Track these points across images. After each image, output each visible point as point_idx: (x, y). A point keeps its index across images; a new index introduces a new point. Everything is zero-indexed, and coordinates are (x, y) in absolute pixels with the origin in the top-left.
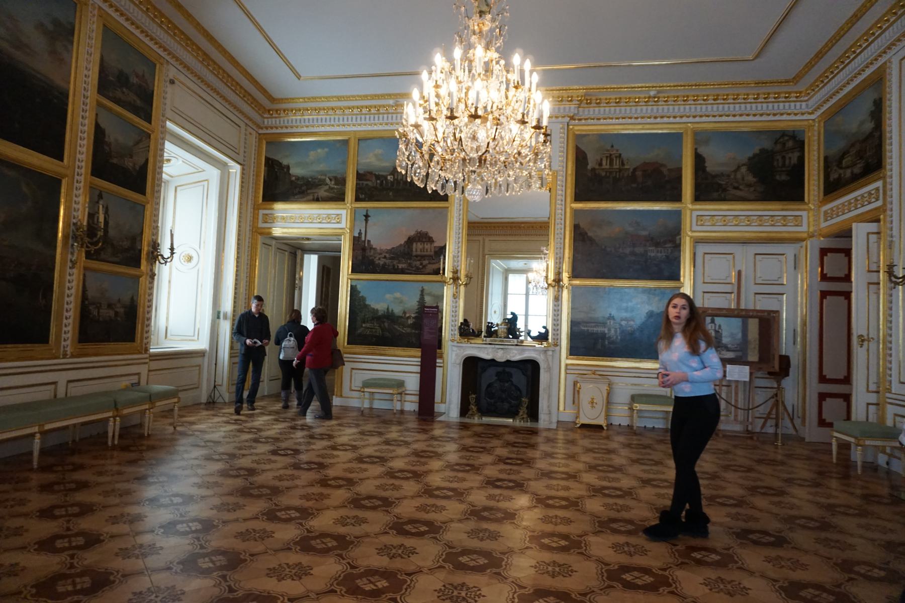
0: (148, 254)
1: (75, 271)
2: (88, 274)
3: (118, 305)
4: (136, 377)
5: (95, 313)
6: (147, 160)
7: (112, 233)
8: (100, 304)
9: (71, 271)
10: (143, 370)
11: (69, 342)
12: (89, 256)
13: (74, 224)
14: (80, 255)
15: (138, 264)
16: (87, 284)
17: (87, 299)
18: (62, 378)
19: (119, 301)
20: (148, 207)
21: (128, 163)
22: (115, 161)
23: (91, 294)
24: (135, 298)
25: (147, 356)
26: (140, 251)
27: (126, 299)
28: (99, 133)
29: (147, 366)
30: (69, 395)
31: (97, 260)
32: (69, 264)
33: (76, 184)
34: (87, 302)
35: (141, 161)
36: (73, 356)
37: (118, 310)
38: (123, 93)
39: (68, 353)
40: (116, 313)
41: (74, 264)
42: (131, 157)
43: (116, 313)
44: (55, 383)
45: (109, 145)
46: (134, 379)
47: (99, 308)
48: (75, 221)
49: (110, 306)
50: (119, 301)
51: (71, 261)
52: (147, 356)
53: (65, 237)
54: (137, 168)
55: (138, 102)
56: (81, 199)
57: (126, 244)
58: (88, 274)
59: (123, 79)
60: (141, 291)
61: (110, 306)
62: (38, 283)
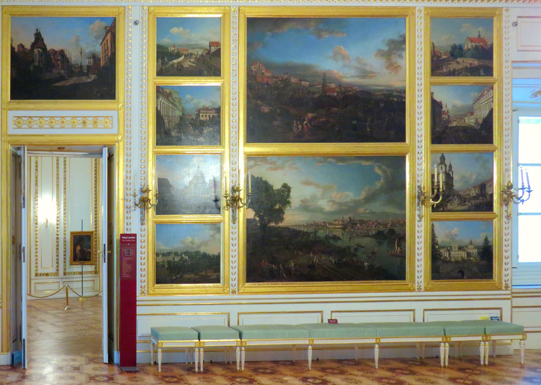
0: (501, 196)
1: (423, 223)
2: (436, 224)
3: (470, 247)
4: (499, 311)
5: (446, 255)
6: (491, 112)
7: (457, 185)
8: (451, 247)
9: (419, 224)
10: (506, 305)
11: (422, 279)
12: (435, 209)
13: (419, 187)
14: (426, 211)
15: (489, 207)
16: (436, 232)
17: (437, 244)
18: (419, 307)
19: (471, 243)
20: (496, 154)
21: (470, 121)
22: (454, 124)
23: (440, 239)
24: (489, 239)
25: (509, 292)
26: (492, 196)
27: (480, 241)
28: (436, 107)
29: (509, 301)
30: (426, 321)
31: (444, 211)
32: (417, 218)
33: (417, 155)
34: (437, 247)
35: (486, 113)
36: (426, 290)
37: (470, 251)
38: (458, 63)
39: (422, 287)
40: (469, 254)
41: (420, 217)
42: (472, 114)
43: (469, 254)
44: (413, 310)
45: (447, 113)
46: (496, 313)
47: (449, 251)
48: (419, 184)
49: (460, 248)
50: (471, 243)
51: (419, 216)
52: (509, 292)
53: (412, 198)
54: (480, 121)
55: (476, 63)
56: (424, 166)
57: (474, 193)
58: (436, 224)
59: (457, 52)
60: (496, 233)
61: (460, 248)
62: (394, 236)
